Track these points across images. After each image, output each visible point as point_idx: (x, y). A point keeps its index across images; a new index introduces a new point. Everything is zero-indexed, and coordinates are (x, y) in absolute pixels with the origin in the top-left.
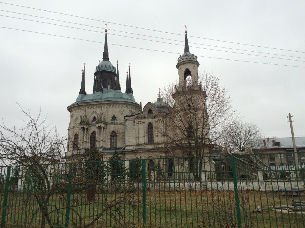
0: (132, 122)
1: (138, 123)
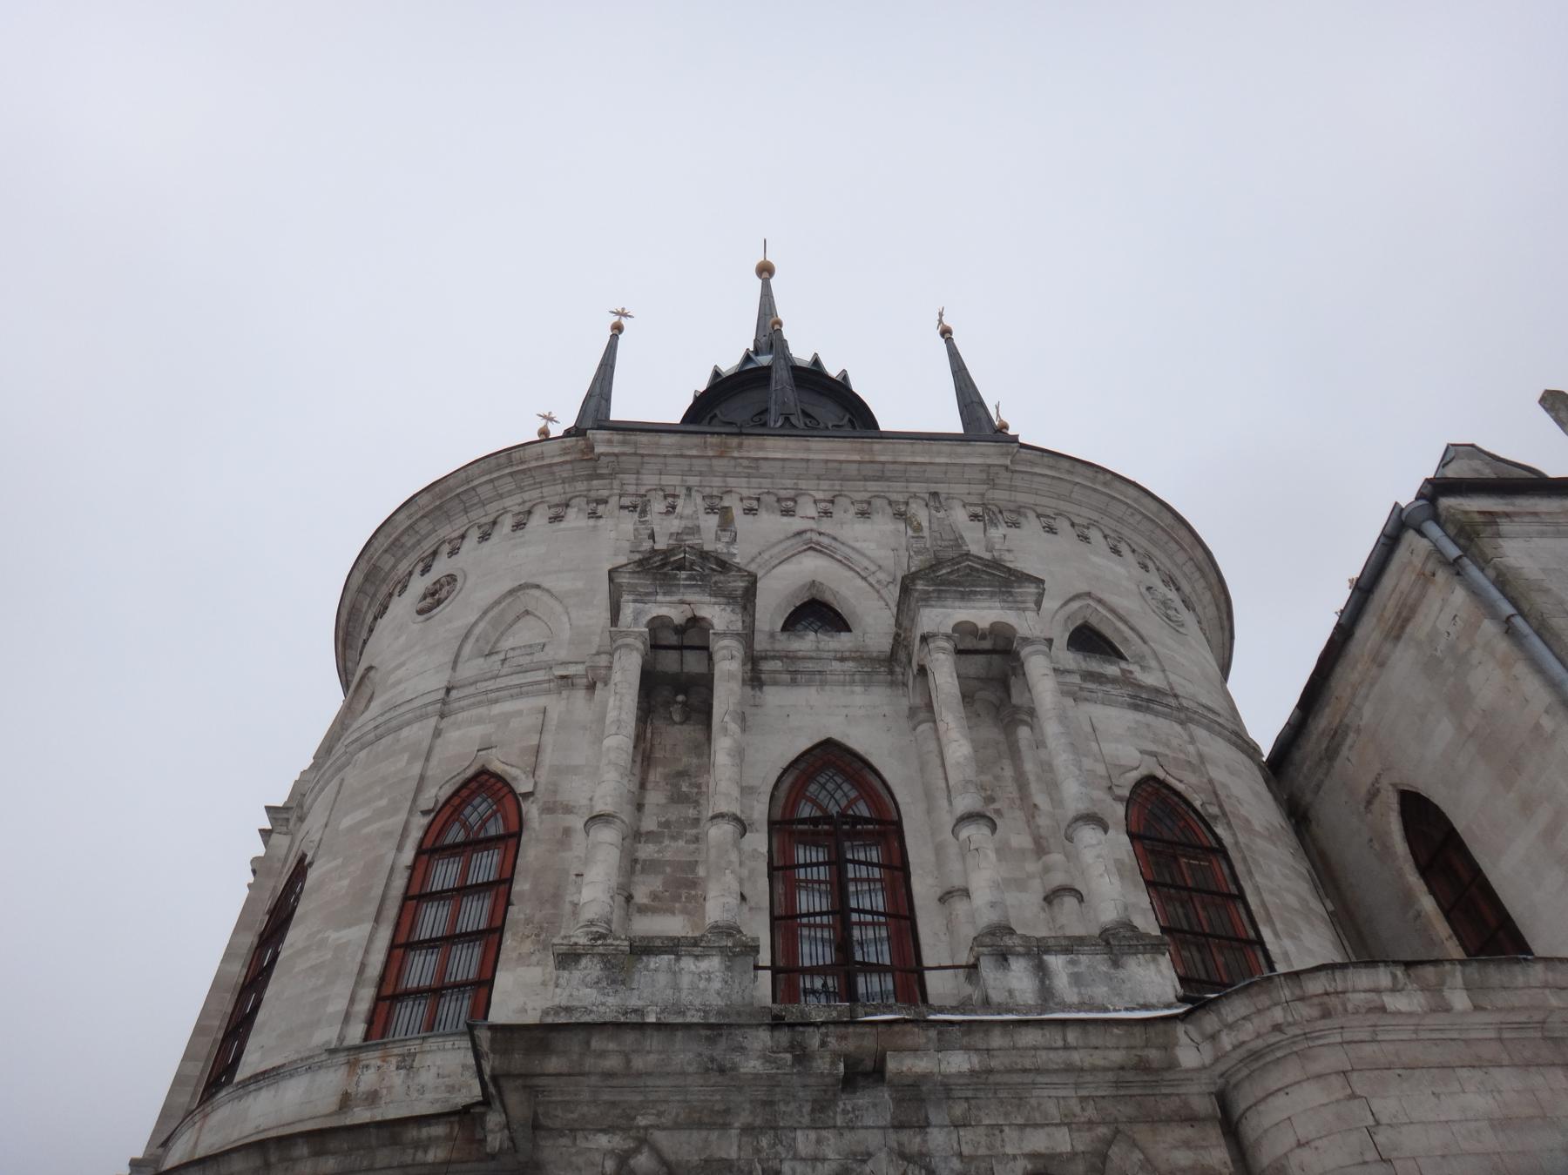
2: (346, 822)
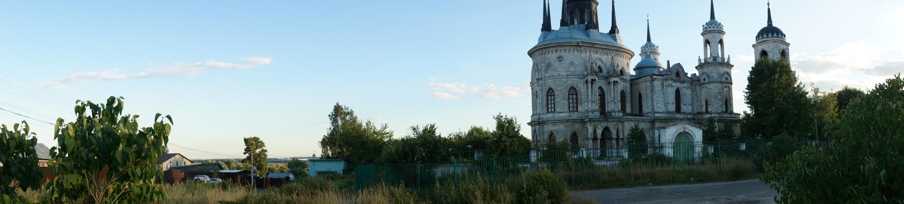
0: (660, 82)
1: (667, 86)
2: (559, 88)
